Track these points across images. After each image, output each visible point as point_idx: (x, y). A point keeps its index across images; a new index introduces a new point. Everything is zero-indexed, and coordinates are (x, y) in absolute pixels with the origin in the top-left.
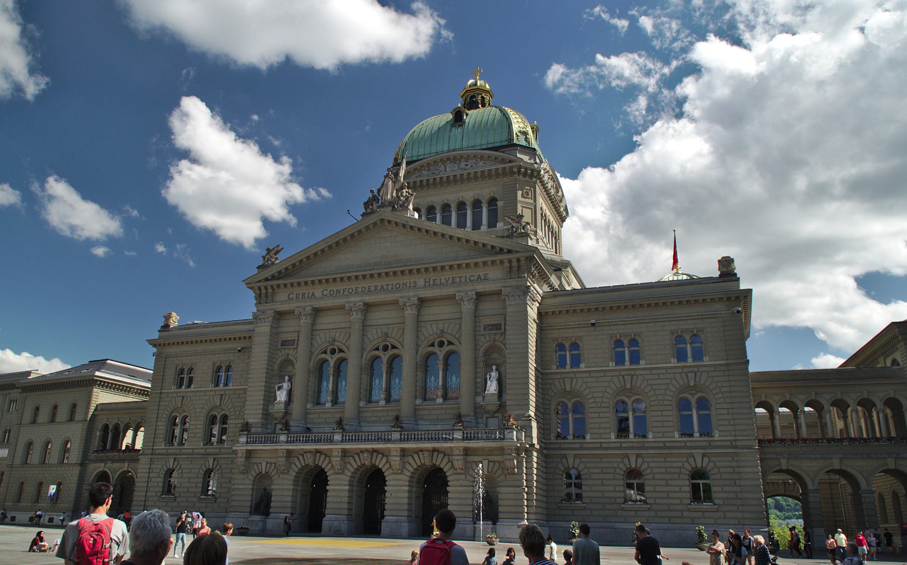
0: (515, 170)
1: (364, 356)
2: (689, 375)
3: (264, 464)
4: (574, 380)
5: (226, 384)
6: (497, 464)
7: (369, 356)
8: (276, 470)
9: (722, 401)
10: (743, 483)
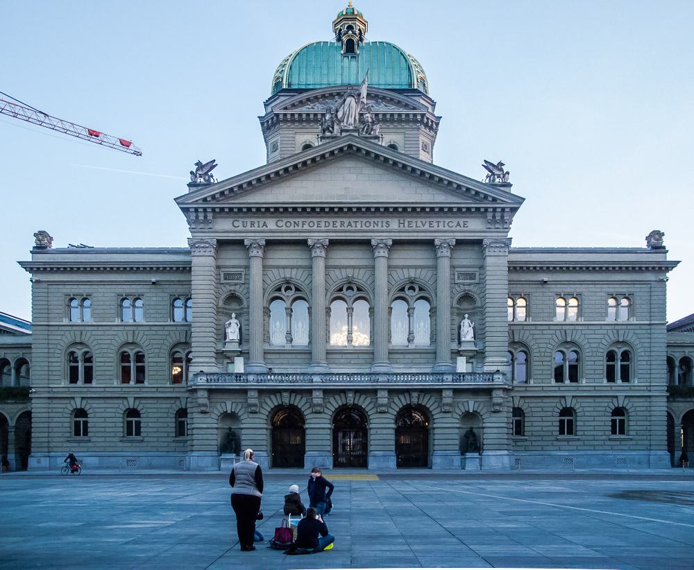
0: (419, 117)
1: (328, 297)
2: (620, 332)
3: (229, 404)
4: (522, 332)
5: (135, 321)
6: (482, 405)
7: (332, 297)
8: (243, 410)
9: (643, 354)
10: (653, 418)
